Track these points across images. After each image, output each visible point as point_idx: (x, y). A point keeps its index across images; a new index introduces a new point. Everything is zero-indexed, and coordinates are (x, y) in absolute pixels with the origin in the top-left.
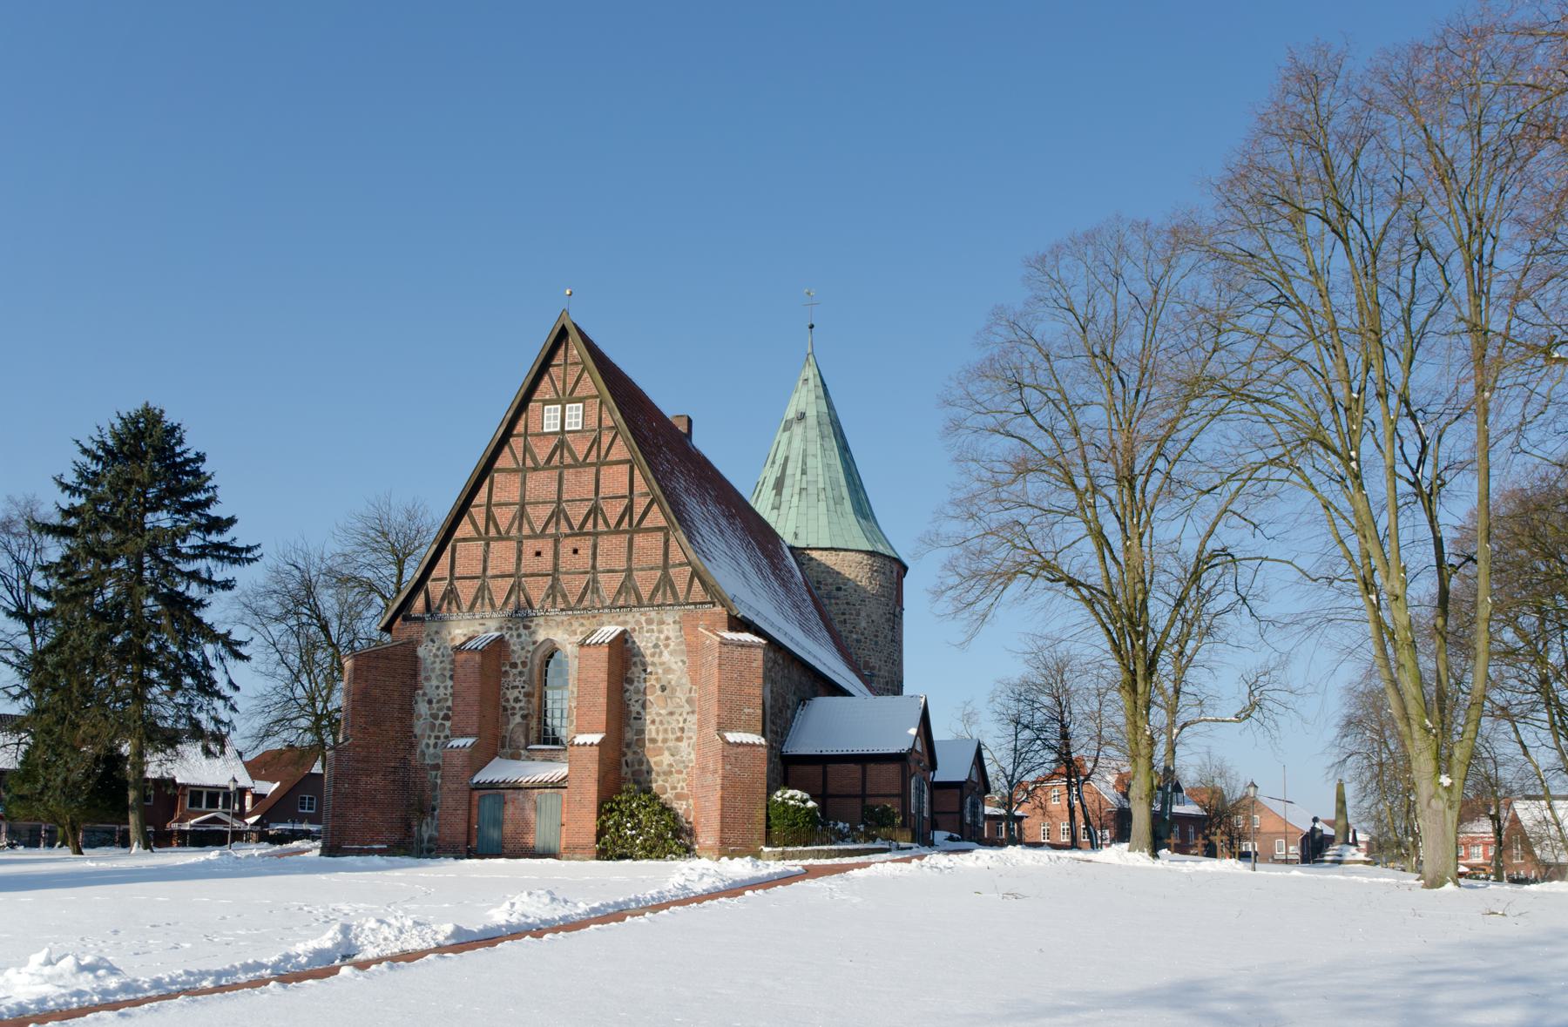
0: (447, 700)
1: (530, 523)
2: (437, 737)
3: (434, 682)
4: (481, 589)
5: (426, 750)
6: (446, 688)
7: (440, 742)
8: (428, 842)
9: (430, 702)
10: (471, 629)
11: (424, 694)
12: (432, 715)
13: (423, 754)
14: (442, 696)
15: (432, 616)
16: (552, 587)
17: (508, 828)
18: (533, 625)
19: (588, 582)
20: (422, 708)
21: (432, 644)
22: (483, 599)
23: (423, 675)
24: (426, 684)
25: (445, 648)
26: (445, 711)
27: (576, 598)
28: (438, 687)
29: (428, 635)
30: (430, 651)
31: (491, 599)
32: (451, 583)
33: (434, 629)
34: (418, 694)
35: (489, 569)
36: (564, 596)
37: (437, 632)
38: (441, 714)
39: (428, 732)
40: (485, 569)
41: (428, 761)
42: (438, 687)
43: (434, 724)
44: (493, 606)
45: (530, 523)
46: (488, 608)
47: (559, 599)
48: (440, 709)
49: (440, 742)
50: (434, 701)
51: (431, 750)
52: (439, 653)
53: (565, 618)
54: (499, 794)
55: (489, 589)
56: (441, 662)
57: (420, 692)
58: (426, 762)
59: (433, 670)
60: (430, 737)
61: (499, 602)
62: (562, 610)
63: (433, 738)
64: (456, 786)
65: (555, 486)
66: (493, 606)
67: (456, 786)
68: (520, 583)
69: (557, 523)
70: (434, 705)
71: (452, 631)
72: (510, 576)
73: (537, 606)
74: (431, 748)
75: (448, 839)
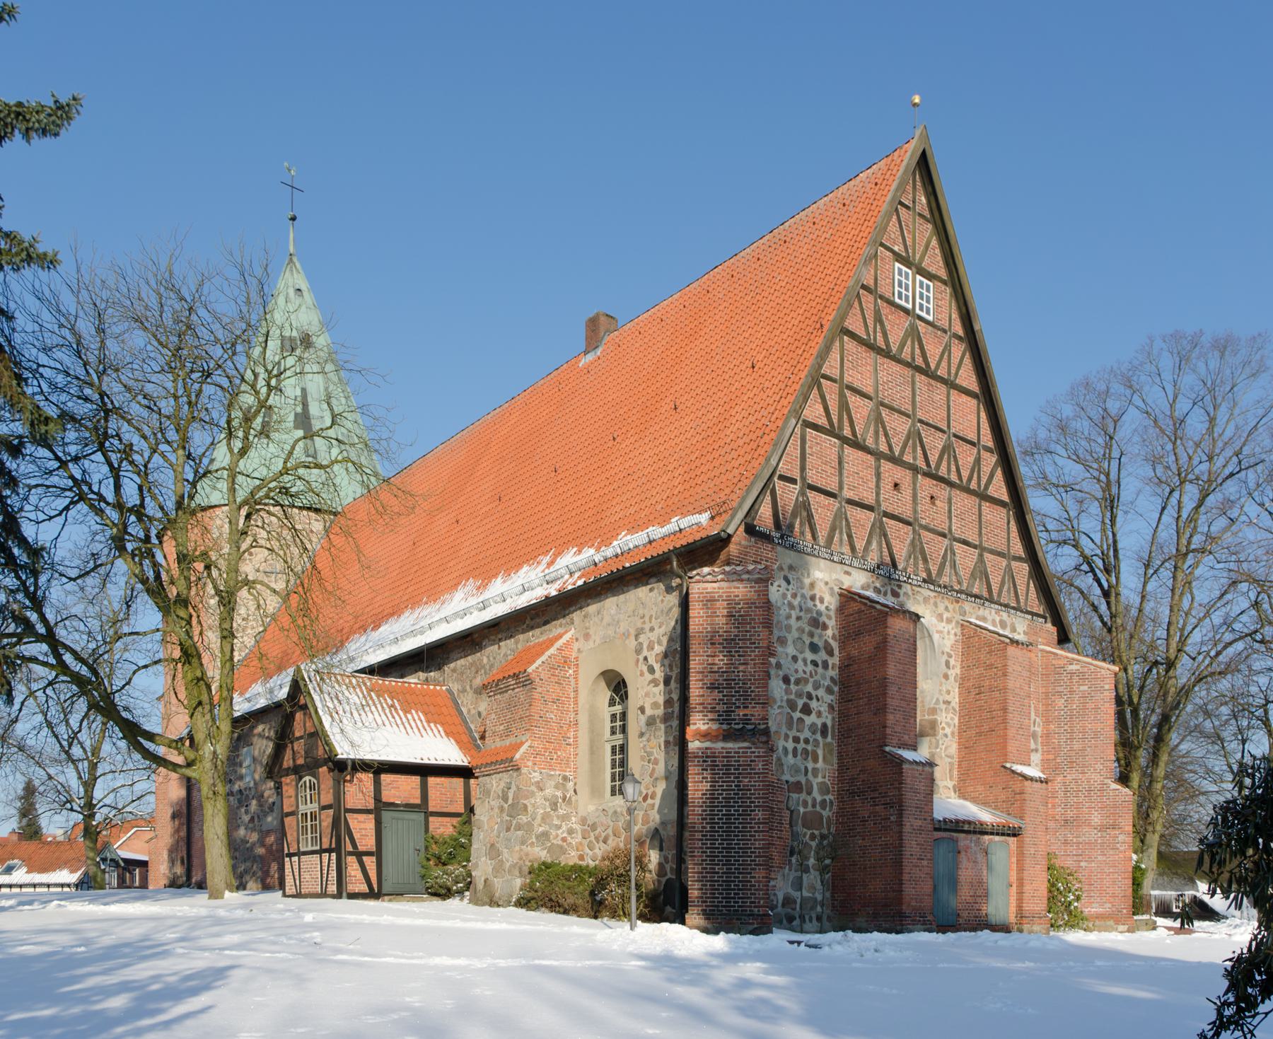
0: (806, 681)
1: (886, 435)
2: (796, 740)
3: (791, 650)
4: (840, 516)
5: (784, 760)
6: (805, 660)
7: (801, 746)
8: (783, 905)
9: (786, 680)
10: (834, 576)
11: (779, 666)
12: (789, 701)
13: (780, 764)
14: (801, 674)
15: (782, 537)
16: (913, 543)
17: (965, 893)
18: (901, 592)
19: (946, 550)
20: (777, 688)
21: (784, 584)
22: (841, 533)
23: (776, 633)
24: (780, 649)
25: (803, 596)
26: (805, 700)
27: (936, 567)
28: (795, 659)
29: (781, 568)
30: (784, 596)
31: (850, 536)
32: (802, 493)
33: (789, 561)
34: (770, 664)
35: (846, 487)
36: (925, 560)
37: (791, 568)
38: (800, 703)
39: (784, 730)
40: (841, 487)
41: (786, 777)
42: (795, 659)
43: (792, 717)
44: (853, 548)
45: (886, 435)
46: (846, 549)
47: (921, 565)
48: (799, 695)
49: (801, 746)
50: (792, 680)
51: (790, 759)
52: (796, 603)
53: (932, 594)
54: (952, 839)
55: (847, 520)
56: (799, 618)
57: (773, 661)
58: (785, 778)
59: (789, 628)
60: (787, 737)
61: (860, 545)
62: (924, 581)
63: (791, 740)
64: (920, 823)
65: (908, 393)
66: (853, 548)
67: (920, 823)
68: (881, 522)
69: (914, 451)
70: (792, 686)
71: (812, 572)
72: (870, 508)
73: (900, 567)
74: (790, 756)
75: (913, 904)
